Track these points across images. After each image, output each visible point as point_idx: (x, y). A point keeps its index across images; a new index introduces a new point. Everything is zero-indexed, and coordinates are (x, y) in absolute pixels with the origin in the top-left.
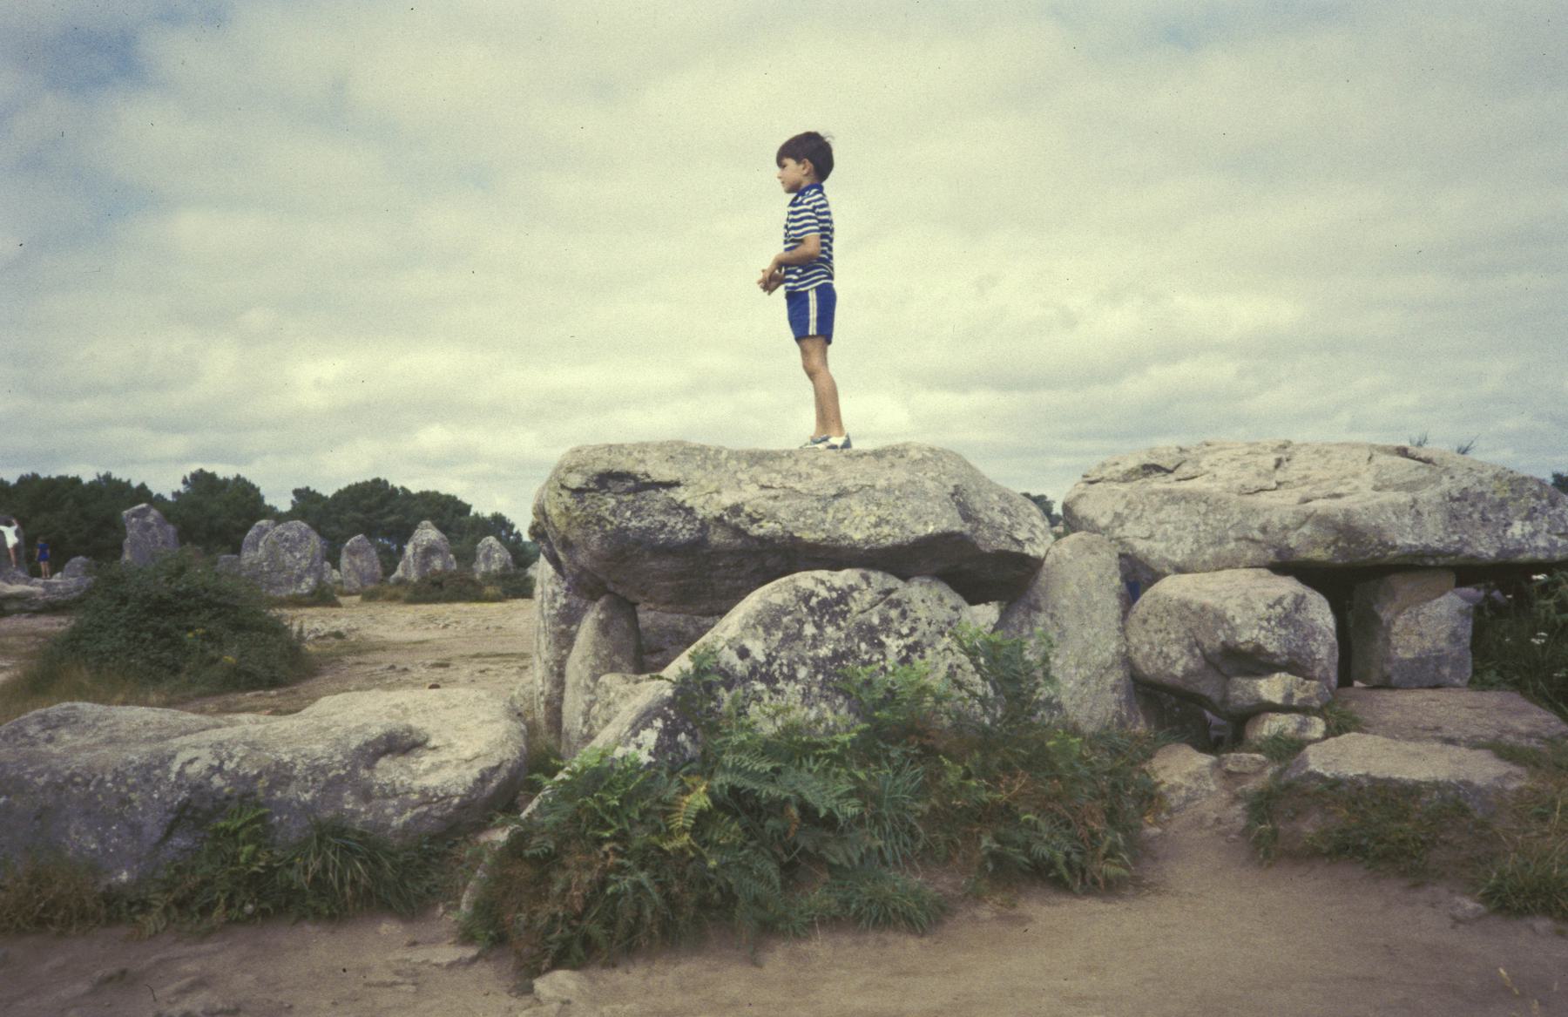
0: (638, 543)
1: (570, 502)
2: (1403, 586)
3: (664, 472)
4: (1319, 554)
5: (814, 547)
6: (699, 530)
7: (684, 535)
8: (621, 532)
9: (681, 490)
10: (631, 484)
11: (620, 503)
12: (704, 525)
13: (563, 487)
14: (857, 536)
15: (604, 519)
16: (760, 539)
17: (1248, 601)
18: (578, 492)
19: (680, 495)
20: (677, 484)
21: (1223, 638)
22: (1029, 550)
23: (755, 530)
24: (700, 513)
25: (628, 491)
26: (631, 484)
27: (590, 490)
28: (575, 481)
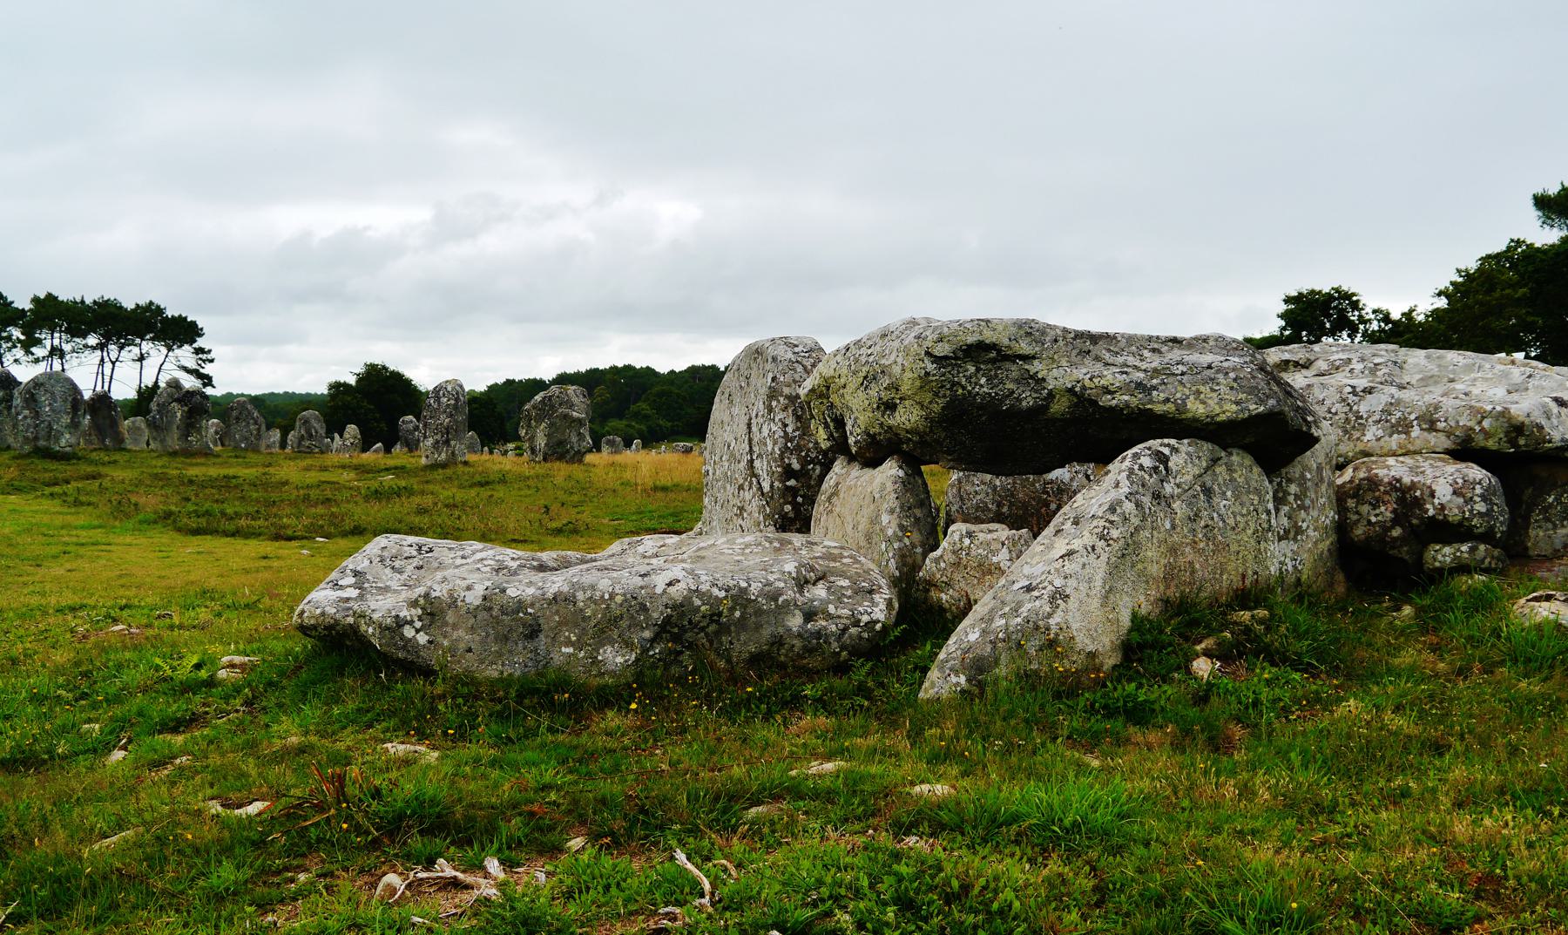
0: (981, 407)
1: (930, 367)
3: (1024, 347)
5: (1162, 417)
9: (1036, 362)
10: (993, 354)
11: (978, 370)
12: (1051, 395)
13: (928, 353)
15: (959, 383)
17: (1447, 484)
18: (937, 360)
19: (1036, 367)
20: (1034, 358)
23: (1106, 401)
26: (993, 354)
27: (956, 358)
28: (942, 350)
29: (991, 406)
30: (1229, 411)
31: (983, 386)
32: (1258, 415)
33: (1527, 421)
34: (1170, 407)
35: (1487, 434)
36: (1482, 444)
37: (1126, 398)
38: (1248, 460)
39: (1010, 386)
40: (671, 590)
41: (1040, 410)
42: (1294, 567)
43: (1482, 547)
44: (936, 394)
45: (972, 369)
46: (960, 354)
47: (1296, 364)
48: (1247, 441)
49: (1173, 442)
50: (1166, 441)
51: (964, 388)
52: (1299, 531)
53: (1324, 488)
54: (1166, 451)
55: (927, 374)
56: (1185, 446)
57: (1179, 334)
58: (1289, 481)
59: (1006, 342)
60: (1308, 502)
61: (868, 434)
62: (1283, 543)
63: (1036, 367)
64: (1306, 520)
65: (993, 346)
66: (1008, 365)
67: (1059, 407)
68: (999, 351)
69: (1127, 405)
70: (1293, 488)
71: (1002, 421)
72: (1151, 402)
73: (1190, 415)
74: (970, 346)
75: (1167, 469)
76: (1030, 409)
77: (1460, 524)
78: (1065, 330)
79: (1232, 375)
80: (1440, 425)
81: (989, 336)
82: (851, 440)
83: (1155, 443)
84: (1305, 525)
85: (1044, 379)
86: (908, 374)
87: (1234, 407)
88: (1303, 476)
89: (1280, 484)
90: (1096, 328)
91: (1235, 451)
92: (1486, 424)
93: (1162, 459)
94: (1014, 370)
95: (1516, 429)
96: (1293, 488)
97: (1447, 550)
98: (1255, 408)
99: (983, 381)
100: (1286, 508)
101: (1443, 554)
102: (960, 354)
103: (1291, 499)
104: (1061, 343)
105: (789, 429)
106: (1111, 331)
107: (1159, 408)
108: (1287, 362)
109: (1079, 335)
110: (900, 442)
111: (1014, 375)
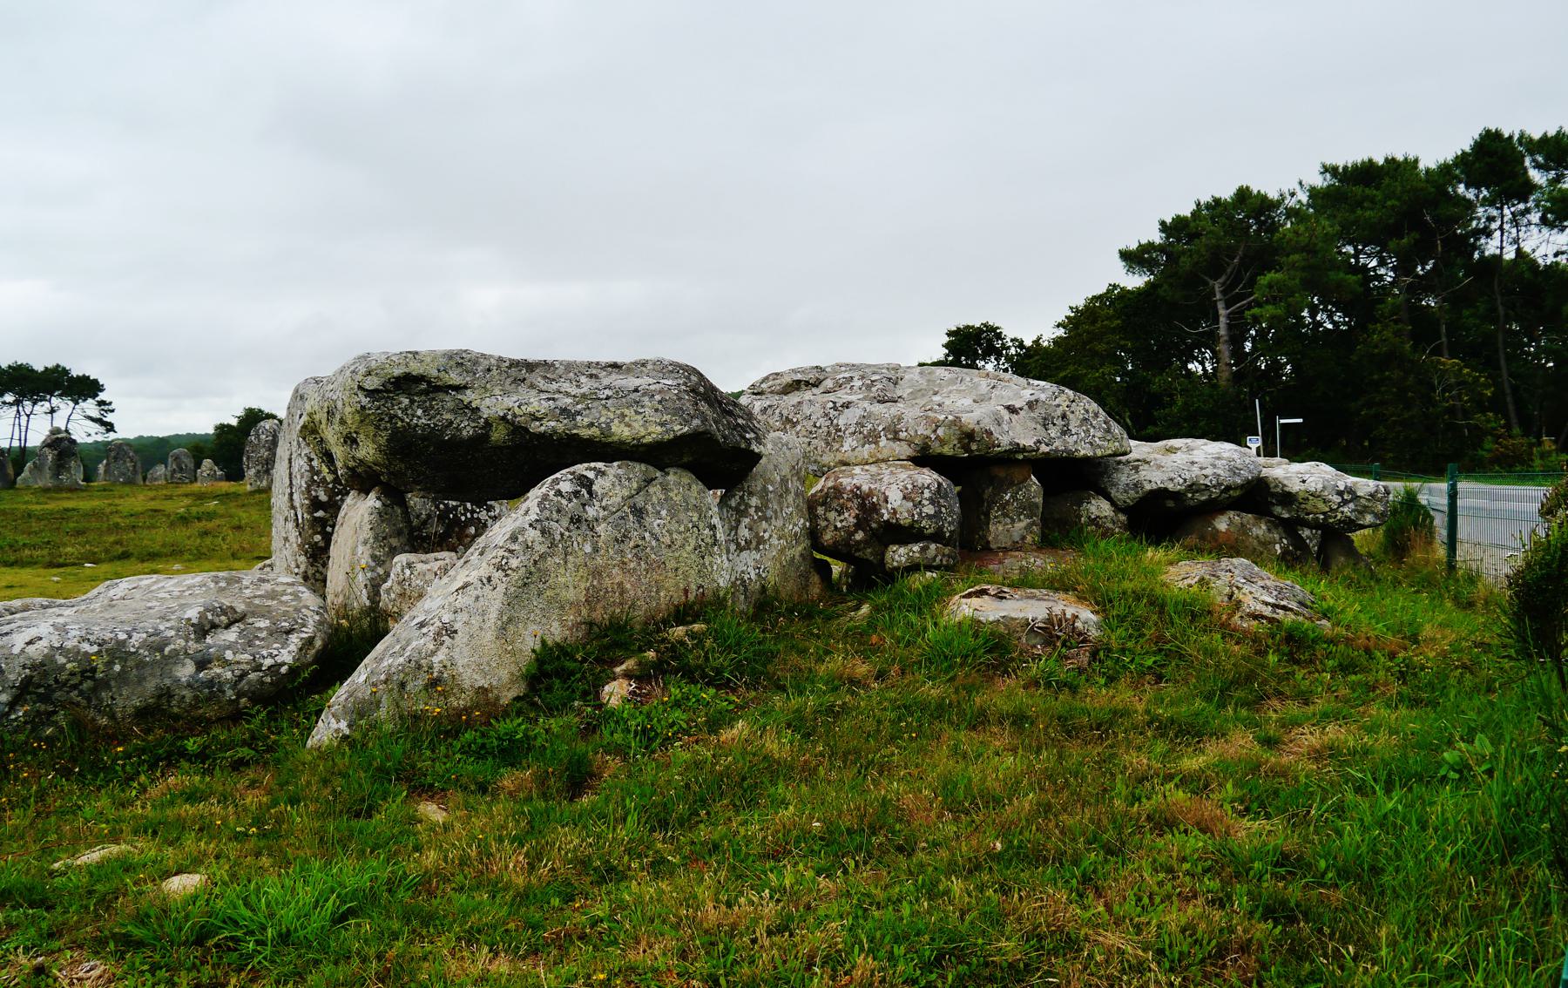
0: (424, 438)
1: (365, 401)
2: (1001, 473)
3: (454, 378)
5: (590, 441)
7: (467, 432)
8: (410, 427)
9: (468, 392)
10: (424, 386)
11: (412, 402)
12: (488, 424)
13: (360, 387)
15: (396, 416)
16: (542, 436)
17: (900, 488)
18: (371, 393)
19: (469, 396)
20: (465, 387)
22: (755, 448)
23: (535, 427)
24: (485, 413)
25: (421, 393)
26: (424, 386)
27: (388, 391)
28: (372, 383)
29: (432, 436)
30: (654, 433)
31: (420, 418)
32: (683, 435)
33: (977, 428)
34: (595, 431)
35: (943, 442)
37: (553, 424)
38: (687, 478)
39: (448, 416)
40: (31, 649)
41: (481, 439)
42: (758, 575)
43: (933, 546)
44: (377, 427)
45: (406, 401)
46: (390, 387)
47: (807, 383)
48: (685, 460)
49: (600, 465)
50: (593, 465)
52: (761, 541)
53: (790, 498)
54: (591, 475)
55: (363, 408)
56: (614, 469)
57: (619, 360)
58: (751, 494)
59: (434, 373)
60: (769, 513)
62: (745, 554)
63: (469, 396)
64: (767, 530)
65: (420, 378)
66: (441, 396)
67: (498, 435)
68: (429, 382)
69: (554, 431)
70: (754, 501)
71: (438, 451)
72: (576, 427)
73: (616, 438)
74: (398, 379)
75: (590, 493)
76: (471, 439)
77: (911, 526)
78: (501, 359)
79: (658, 397)
81: (415, 368)
83: (580, 468)
84: (766, 536)
85: (478, 409)
86: (348, 409)
87: (659, 429)
88: (765, 488)
89: (742, 498)
90: (533, 356)
91: (671, 471)
92: (940, 432)
93: (586, 483)
94: (449, 400)
95: (968, 436)
96: (754, 501)
97: (902, 550)
98: (680, 429)
99: (419, 412)
100: (747, 520)
101: (899, 555)
102: (390, 387)
103: (752, 511)
104: (495, 372)
105: (315, 463)
106: (550, 359)
107: (585, 433)
108: (799, 382)
109: (515, 364)
110: (378, 475)
111: (450, 405)
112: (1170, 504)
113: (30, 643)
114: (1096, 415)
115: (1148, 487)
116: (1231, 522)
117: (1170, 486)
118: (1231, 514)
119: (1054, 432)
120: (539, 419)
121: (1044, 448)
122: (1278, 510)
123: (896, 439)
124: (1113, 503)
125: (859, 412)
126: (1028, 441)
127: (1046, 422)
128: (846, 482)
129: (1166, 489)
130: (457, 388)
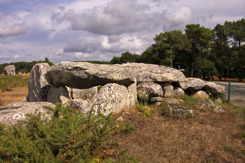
3: (85, 67)
4: (160, 80)
6: (89, 77)
9: (87, 70)
10: (79, 69)
11: (76, 72)
14: (116, 78)
16: (101, 78)
19: (87, 71)
20: (87, 69)
21: (152, 92)
28: (70, 68)
32: (126, 79)
34: (111, 78)
35: (159, 79)
36: (158, 80)
40: (16, 118)
43: (160, 97)
47: (128, 67)
49: (111, 84)
51: (74, 75)
54: (110, 86)
59: (81, 67)
61: (57, 82)
65: (79, 68)
67: (91, 78)
74: (75, 67)
75: (111, 89)
79: (121, 72)
80: (152, 78)
82: (54, 83)
83: (108, 84)
87: (122, 78)
93: (110, 87)
95: (163, 78)
98: (125, 78)
99: (77, 73)
101: (154, 99)
103: (130, 91)
107: (109, 78)
111: (83, 72)
112: (191, 89)
113: (17, 117)
114: (182, 74)
115: (188, 86)
116: (200, 93)
117: (192, 86)
118: (200, 91)
119: (176, 77)
120: (100, 75)
121: (175, 80)
122: (207, 90)
123: (151, 78)
124: (182, 89)
125: (143, 73)
126: (172, 79)
127: (175, 75)
128: (144, 86)
129: (191, 87)
130: (85, 69)
